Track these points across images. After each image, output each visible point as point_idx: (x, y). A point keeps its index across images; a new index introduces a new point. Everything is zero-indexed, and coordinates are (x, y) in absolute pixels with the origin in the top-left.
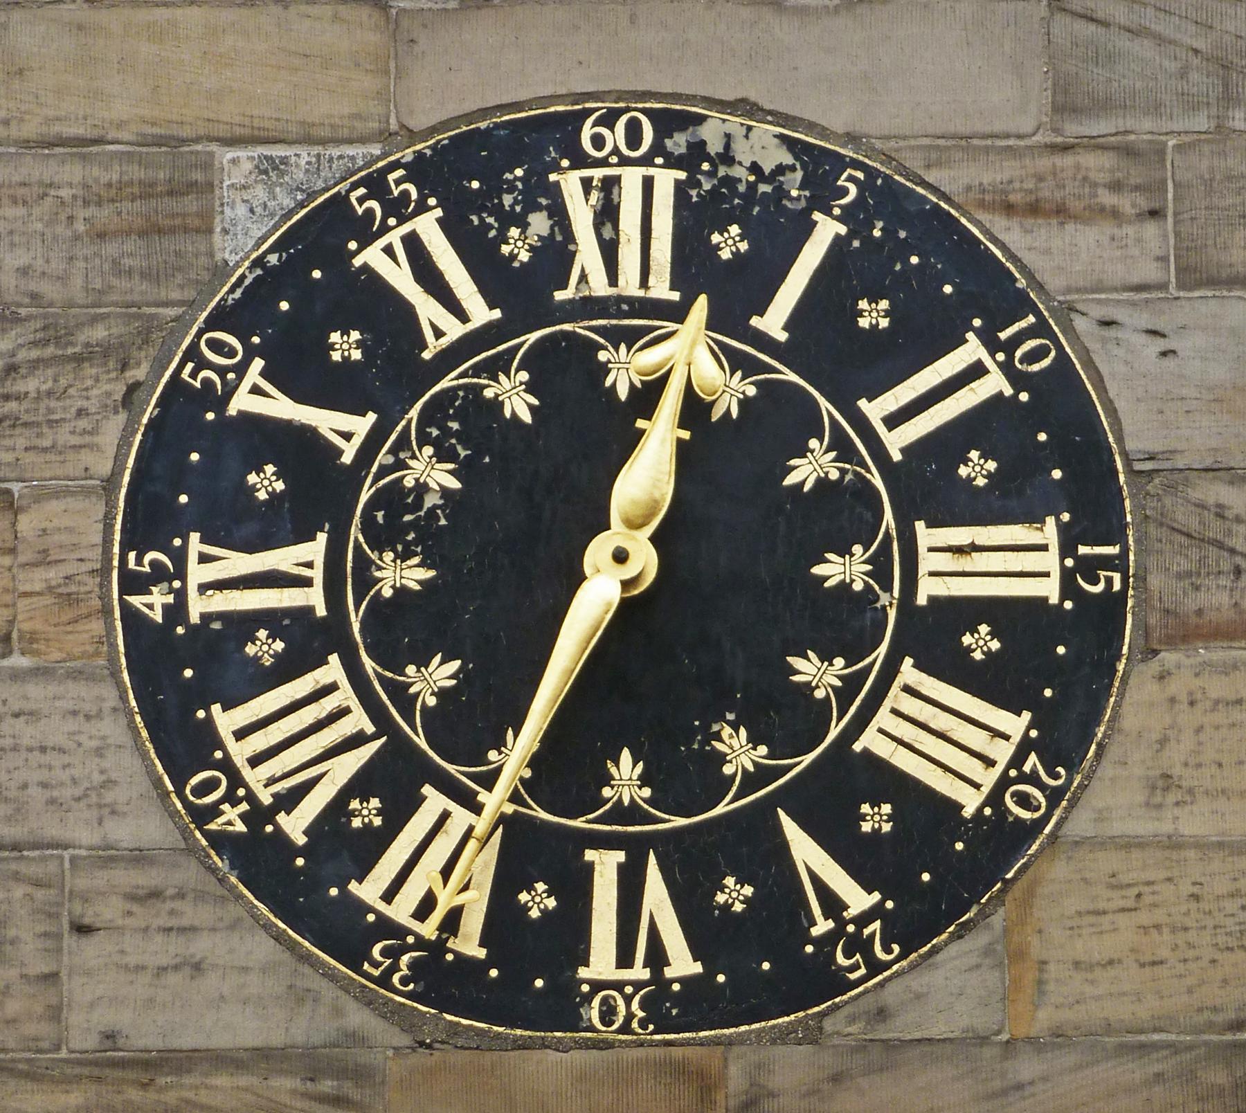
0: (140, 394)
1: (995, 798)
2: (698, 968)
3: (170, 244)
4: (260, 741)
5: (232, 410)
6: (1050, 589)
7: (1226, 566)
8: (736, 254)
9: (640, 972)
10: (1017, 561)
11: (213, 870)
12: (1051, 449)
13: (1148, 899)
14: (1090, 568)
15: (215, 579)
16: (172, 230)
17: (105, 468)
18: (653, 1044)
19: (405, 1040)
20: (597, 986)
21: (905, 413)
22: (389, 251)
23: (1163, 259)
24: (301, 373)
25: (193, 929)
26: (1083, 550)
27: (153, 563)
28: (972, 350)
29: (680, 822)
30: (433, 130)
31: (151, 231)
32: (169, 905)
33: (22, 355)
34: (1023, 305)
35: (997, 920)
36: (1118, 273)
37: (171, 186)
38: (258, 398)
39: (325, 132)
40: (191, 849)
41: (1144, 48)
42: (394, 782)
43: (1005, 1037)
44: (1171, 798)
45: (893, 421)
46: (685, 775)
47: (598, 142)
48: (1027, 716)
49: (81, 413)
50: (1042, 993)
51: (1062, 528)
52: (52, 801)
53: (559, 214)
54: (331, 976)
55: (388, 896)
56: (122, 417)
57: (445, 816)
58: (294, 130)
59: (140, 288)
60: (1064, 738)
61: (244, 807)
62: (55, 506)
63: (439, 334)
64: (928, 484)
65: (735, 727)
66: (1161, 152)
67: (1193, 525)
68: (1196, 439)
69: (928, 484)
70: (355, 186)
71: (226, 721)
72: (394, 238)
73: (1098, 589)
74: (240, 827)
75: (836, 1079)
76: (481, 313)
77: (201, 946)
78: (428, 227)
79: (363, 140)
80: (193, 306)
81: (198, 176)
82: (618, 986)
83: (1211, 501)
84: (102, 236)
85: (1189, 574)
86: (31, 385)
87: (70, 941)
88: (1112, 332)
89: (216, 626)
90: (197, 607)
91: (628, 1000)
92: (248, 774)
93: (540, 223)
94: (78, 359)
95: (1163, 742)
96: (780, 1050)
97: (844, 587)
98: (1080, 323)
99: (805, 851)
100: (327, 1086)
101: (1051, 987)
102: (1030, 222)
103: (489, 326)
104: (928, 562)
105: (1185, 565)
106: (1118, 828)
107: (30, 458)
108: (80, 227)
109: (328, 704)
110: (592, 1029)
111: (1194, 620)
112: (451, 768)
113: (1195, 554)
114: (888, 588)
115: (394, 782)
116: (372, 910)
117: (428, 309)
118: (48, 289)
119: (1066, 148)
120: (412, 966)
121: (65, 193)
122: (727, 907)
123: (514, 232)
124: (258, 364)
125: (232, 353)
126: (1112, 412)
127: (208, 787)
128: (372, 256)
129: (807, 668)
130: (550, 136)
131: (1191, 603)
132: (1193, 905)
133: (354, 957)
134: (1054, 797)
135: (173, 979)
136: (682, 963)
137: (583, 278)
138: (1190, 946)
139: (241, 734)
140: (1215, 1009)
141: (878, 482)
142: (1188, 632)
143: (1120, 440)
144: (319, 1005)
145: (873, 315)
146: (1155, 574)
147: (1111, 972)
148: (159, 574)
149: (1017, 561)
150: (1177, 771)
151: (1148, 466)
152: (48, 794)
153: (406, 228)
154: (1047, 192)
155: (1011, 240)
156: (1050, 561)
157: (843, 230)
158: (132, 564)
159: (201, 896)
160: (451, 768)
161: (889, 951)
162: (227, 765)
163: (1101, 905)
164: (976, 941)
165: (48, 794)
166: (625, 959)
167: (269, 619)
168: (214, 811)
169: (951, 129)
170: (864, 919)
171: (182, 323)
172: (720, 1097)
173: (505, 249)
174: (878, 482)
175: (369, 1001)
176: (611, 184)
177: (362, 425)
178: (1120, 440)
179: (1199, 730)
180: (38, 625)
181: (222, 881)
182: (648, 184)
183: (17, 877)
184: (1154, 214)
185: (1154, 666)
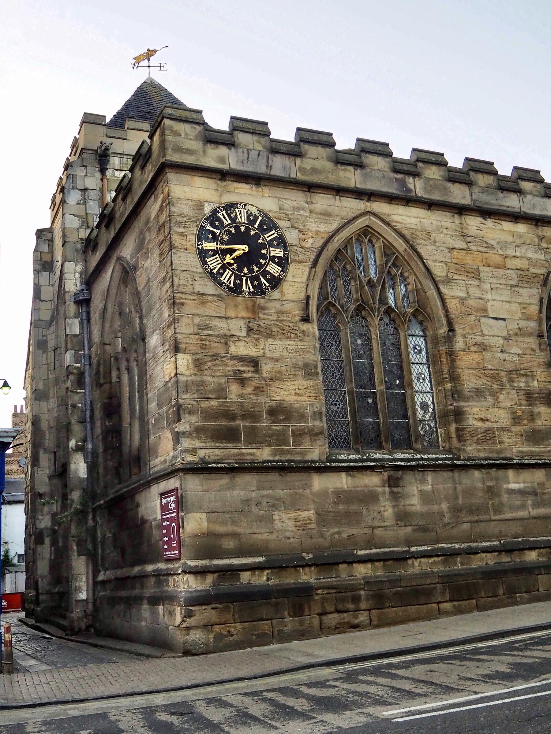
1: (279, 276)
4: (211, 263)
6: (282, 256)
10: (278, 252)
12: (281, 242)
14: (286, 254)
28: (274, 231)
37: (200, 206)
38: (209, 227)
42: (224, 267)
53: (236, 213)
60: (284, 270)
68: (294, 242)
69: (271, 243)
71: (208, 260)
72: (221, 213)
76: (230, 222)
77: (207, 283)
78: (224, 212)
80: (203, 218)
93: (234, 214)
104: (271, 252)
117: (225, 221)
118: (189, 215)
128: (219, 215)
129: (261, 261)
136: (252, 290)
142: (295, 261)
144: (219, 291)
155: (276, 221)
156: (282, 253)
164: (278, 290)
166: (246, 289)
175: (223, 290)
177: (219, 231)
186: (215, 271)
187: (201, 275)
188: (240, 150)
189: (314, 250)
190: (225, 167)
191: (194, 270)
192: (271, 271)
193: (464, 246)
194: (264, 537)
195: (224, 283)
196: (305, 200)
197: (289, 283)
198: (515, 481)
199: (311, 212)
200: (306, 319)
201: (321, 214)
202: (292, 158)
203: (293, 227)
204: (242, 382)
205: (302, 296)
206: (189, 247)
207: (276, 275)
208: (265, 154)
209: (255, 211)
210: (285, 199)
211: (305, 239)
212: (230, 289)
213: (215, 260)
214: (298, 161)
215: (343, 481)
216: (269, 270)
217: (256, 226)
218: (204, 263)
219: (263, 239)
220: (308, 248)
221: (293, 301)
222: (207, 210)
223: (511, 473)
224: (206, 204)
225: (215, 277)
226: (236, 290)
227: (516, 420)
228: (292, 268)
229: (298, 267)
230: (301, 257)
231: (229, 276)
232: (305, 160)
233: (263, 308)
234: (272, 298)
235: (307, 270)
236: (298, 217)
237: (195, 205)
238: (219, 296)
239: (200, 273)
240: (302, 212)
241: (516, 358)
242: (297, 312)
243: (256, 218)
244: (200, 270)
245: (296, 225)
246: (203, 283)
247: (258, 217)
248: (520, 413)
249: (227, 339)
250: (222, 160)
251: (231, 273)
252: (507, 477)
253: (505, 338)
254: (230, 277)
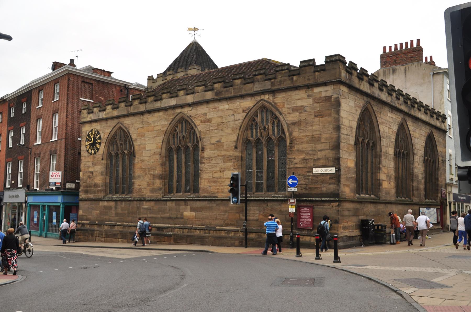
193: (141, 126)
194: (90, 217)
198: (146, 205)
204: (90, 178)
215: (106, 204)
223: (144, 202)
226: (91, 154)
227: (149, 185)
238: (88, 156)
241: (152, 164)
248: (150, 183)
249: (89, 167)
252: (143, 204)
253: (150, 157)
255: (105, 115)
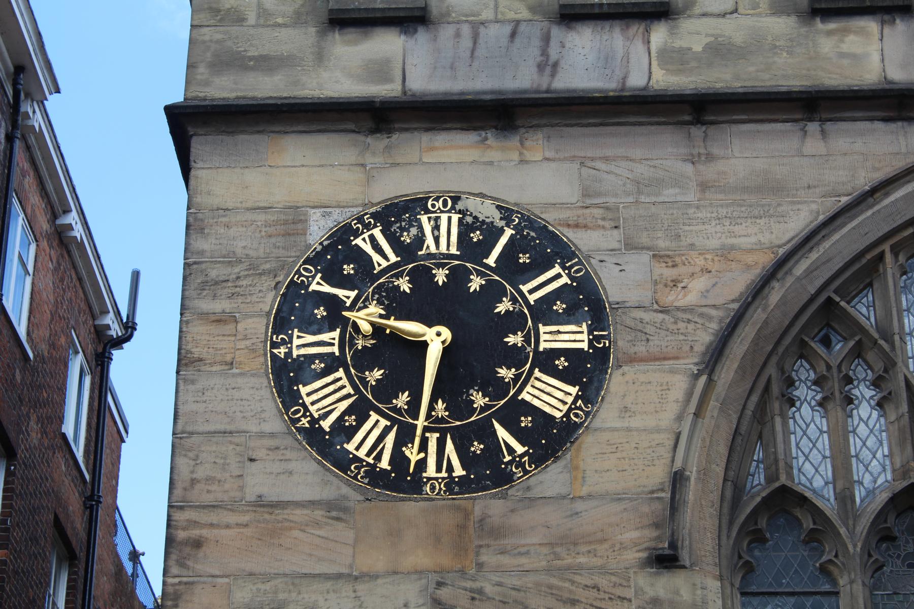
0: (280, 285)
1: (567, 415)
2: (464, 473)
3: (292, 238)
4: (315, 397)
5: (310, 290)
6: (585, 346)
7: (644, 338)
8: (479, 240)
9: (444, 474)
10: (573, 337)
11: (297, 440)
12: (584, 301)
13: (620, 449)
14: (598, 339)
15: (302, 344)
16: (294, 234)
17: (267, 309)
18: (448, 499)
19: (361, 498)
20: (429, 479)
21: (535, 289)
22: (364, 240)
23: (620, 241)
24: (333, 276)
25: (290, 460)
26: (595, 333)
27: (282, 339)
28: (557, 269)
29: (458, 423)
30: (379, 203)
31: (287, 234)
32: (282, 452)
33: (242, 273)
34: (573, 255)
35: (568, 456)
36: (605, 245)
38: (318, 285)
39: (345, 204)
40: (290, 433)
41: (611, 177)
42: (360, 410)
43: (571, 496)
44: (628, 414)
45: (531, 292)
46: (460, 407)
47: (433, 206)
48: (577, 388)
49: (260, 291)
50: (584, 481)
51: (588, 326)
52: (244, 417)
53: (420, 228)
54: (337, 476)
55: (357, 449)
56: (274, 292)
57: (378, 421)
58: (334, 204)
59: (282, 252)
60: (590, 393)
61: (309, 419)
62: (250, 320)
63: (379, 265)
64: (543, 312)
65: (478, 391)
66: (618, 209)
67: (632, 324)
68: (632, 296)
69: (543, 312)
70: (353, 220)
71: (304, 390)
72: (366, 236)
73: (601, 345)
74: (307, 425)
75: (512, 511)
76: (393, 258)
77: (292, 466)
78: (377, 232)
79: (356, 206)
80: (299, 257)
81: (303, 218)
82: (436, 479)
83: (638, 317)
84: (270, 236)
85: (631, 341)
86: (244, 283)
87: (248, 463)
88: (603, 264)
89: (302, 359)
90: (295, 353)
91: (440, 484)
92: (311, 408)
93: (414, 231)
94: (260, 274)
95: (624, 396)
96: (493, 501)
97: (515, 345)
98: (592, 261)
99: (502, 433)
100: (334, 514)
101: (587, 479)
102: (575, 230)
103: (396, 262)
104: (543, 337)
105: (630, 338)
106: (608, 425)
107: (243, 305)
108: (263, 234)
109: (339, 384)
110: (427, 494)
111: (633, 355)
112: (380, 406)
113: (633, 335)
114: (530, 346)
115: (360, 410)
116: (351, 453)
117: (376, 258)
118: (252, 253)
119: (587, 207)
120: (365, 472)
121: (259, 223)
122: (475, 452)
123: (405, 234)
124: (319, 275)
125: (311, 271)
126: (604, 289)
127: (298, 411)
128: (358, 241)
129: (503, 372)
130: (418, 204)
131: (632, 350)
132: (636, 451)
133: (345, 469)
134: (587, 414)
135: (282, 477)
136: (459, 471)
137: (428, 247)
138: (636, 465)
139: (308, 394)
140: (644, 486)
141: (526, 311)
142: (633, 360)
143: (607, 298)
144: (334, 486)
145: (524, 259)
146: (622, 341)
147: (608, 473)
148: (283, 342)
149: (573, 337)
150: (629, 406)
151: (616, 306)
152: (242, 415)
153: (370, 233)
154: (581, 221)
155: (569, 235)
156: (585, 336)
157: (514, 232)
158: (274, 339)
159: (292, 448)
160: (380, 406)
161: (530, 467)
162: (304, 405)
163: (604, 451)
164: (561, 464)
165: (242, 415)
166: (439, 470)
167: (320, 356)
168: (299, 420)
169: (549, 202)
170: (522, 456)
171: (295, 263)
172: (472, 517)
173: (402, 239)
174: (526, 311)
175: (349, 484)
176: (437, 219)
177: (353, 294)
178: (607, 298)
179: (637, 392)
180: (242, 359)
181: (300, 443)
182: (450, 219)
183: (231, 442)
184: (616, 227)
185: (621, 371)
186: (326, 424)
187: (272, 443)
188: (446, 32)
189: (713, 312)
190: (389, 90)
191: (253, 428)
192: (536, 403)
195: (357, 459)
196: (683, 151)
197: (606, 436)
199: (704, 187)
200: (666, 560)
201: (746, 189)
202: (637, 28)
203: (631, 246)
205: (658, 475)
206: (240, 356)
207: (558, 415)
208: (533, 32)
209: (488, 212)
210: (606, 159)
211: (675, 282)
212: (375, 477)
213: (331, 388)
214: (659, 34)
216: (528, 398)
217: (491, 261)
218: (289, 397)
219: (514, 300)
220: (685, 310)
221: (617, 498)
222: (318, 231)
224: (315, 216)
225: (326, 443)
228: (618, 382)
229: (642, 378)
230: (660, 342)
231: (376, 433)
232: (687, 25)
233: (497, 532)
234: (536, 492)
235: (679, 385)
236: (653, 209)
237: (276, 223)
238: (336, 509)
239: (272, 435)
240: (669, 194)
242: (634, 538)
243: (493, 234)
244: (274, 423)
245: (644, 240)
246: (277, 467)
247: (501, 231)
250: (379, 70)
251: (384, 423)
254: (381, 438)
255: (673, 58)
